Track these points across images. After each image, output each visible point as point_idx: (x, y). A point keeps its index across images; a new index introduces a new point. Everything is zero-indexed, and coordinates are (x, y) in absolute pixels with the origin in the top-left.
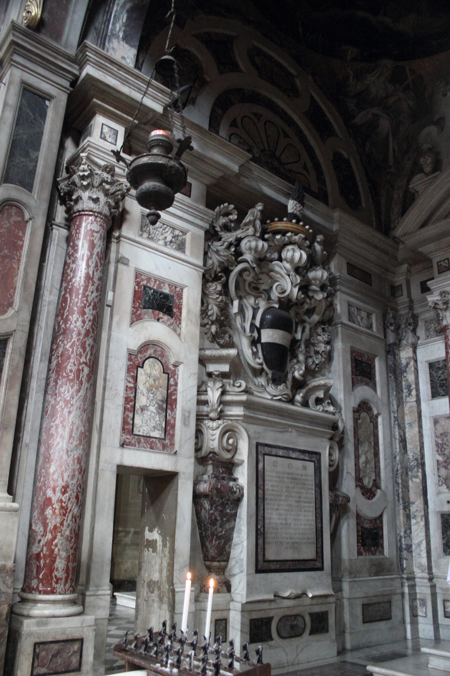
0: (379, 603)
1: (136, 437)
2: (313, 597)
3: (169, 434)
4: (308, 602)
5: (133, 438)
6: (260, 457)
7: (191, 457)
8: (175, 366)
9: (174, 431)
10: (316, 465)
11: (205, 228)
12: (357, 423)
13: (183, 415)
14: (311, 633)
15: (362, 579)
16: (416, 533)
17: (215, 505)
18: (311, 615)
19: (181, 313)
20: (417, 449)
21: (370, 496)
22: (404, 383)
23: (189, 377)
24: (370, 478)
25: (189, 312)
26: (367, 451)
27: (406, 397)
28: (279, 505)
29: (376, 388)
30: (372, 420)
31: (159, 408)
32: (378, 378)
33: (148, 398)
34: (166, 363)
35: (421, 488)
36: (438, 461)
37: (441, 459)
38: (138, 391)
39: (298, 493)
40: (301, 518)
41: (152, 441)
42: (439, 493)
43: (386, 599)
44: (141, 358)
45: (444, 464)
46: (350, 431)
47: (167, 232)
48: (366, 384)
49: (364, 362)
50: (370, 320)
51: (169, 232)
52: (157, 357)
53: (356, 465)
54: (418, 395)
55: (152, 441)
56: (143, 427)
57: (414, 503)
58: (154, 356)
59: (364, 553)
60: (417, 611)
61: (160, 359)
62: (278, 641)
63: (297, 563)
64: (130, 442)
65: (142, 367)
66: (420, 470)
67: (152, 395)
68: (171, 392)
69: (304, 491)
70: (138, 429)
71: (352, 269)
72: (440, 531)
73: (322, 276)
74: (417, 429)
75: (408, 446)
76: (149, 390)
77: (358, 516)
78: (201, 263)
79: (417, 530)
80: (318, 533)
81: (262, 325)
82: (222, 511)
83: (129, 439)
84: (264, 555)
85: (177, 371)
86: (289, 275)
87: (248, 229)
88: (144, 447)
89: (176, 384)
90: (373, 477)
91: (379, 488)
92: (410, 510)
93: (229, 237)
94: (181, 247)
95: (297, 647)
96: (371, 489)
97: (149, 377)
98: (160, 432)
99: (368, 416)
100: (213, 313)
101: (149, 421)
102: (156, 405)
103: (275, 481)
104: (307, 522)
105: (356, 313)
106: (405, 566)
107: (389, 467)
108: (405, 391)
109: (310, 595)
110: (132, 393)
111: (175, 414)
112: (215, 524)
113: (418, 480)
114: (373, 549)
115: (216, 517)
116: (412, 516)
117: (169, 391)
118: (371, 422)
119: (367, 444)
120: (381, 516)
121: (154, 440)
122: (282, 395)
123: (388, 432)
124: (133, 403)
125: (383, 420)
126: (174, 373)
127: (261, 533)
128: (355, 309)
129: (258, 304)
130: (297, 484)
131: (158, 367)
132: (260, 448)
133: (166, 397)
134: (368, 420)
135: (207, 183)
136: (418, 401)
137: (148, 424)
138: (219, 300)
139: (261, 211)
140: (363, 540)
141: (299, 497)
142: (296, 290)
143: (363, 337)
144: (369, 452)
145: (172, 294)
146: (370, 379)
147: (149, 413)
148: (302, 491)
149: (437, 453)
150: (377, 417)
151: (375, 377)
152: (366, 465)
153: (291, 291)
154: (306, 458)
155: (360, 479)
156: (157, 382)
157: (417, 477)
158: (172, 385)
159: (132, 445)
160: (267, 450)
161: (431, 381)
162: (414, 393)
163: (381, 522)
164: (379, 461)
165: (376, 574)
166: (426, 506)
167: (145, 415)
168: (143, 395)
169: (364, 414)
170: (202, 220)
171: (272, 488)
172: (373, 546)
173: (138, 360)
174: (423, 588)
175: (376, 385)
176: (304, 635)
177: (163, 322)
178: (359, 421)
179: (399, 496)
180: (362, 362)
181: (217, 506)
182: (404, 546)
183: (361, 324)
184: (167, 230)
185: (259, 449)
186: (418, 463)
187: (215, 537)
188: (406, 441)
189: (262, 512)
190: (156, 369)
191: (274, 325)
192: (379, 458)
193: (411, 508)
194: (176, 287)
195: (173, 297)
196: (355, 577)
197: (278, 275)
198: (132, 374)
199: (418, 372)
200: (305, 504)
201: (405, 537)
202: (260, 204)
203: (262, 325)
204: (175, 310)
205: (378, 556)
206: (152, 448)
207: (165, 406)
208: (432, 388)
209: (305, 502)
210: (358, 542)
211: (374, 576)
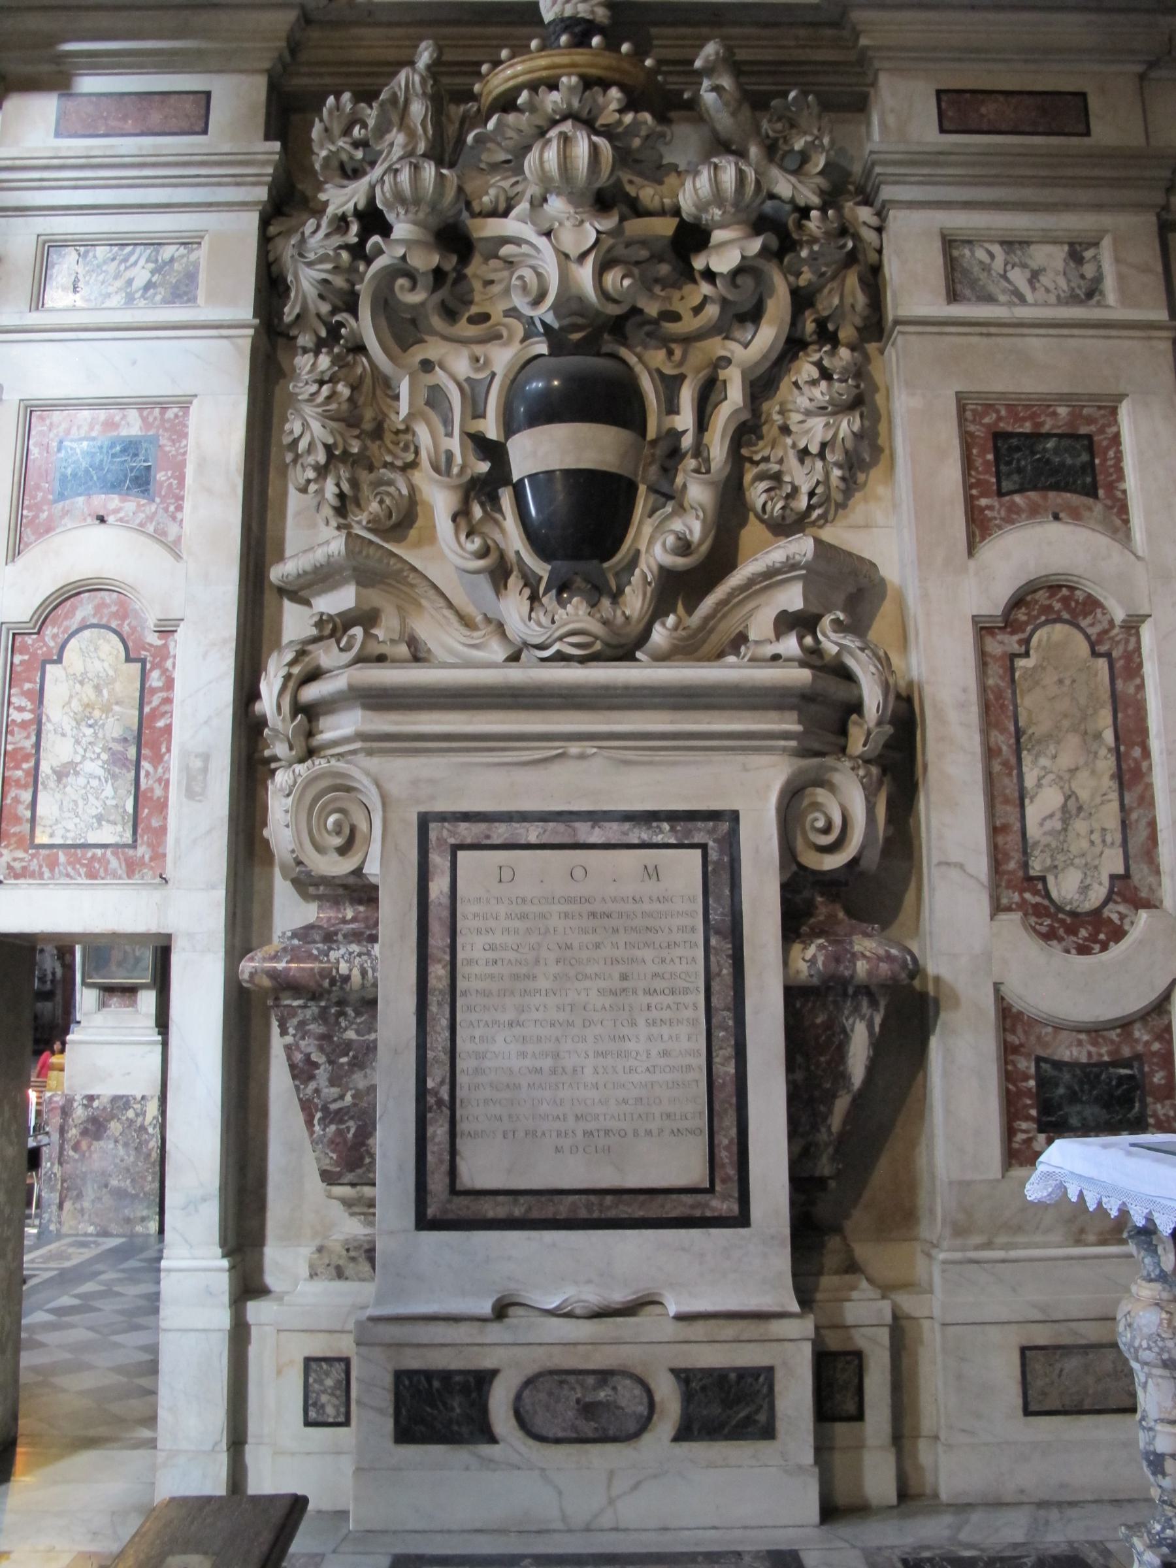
1: (43, 852)
2: (681, 1318)
3: (149, 828)
4: (671, 1330)
5: (33, 856)
6: (439, 861)
7: (213, 887)
8: (166, 630)
9: (165, 818)
10: (713, 855)
11: (256, 203)
12: (1012, 669)
13: (186, 769)
14: (684, 1434)
15: (1013, 1254)
17: (295, 1021)
18: (684, 1376)
19: (181, 479)
21: (1093, 938)
23: (205, 655)
24: (1090, 869)
25: (202, 464)
26: (1073, 771)
28: (522, 1009)
29: (1126, 522)
30: (1103, 648)
31: (114, 763)
32: (1132, 482)
33: (78, 742)
34: (133, 629)
38: (47, 727)
39: (615, 961)
40: (631, 1046)
41: (94, 856)
44: (54, 637)
46: (962, 706)
47: (136, 263)
48: (1056, 517)
49: (1049, 436)
50: (1089, 270)
51: (142, 262)
52: (104, 621)
53: (995, 830)
55: (94, 856)
56: (64, 823)
58: (95, 621)
61: (114, 625)
62: (523, 1449)
63: (609, 1199)
64: (24, 868)
65: (59, 660)
67: (90, 731)
68: (153, 710)
69: (648, 954)
70: (49, 830)
71: (958, 109)
73: (716, 183)
76: (83, 718)
78: (245, 311)
80: (719, 1096)
81: (510, 427)
82: (326, 1037)
83: (22, 860)
84: (453, 1172)
85: (171, 645)
86: (548, 234)
87: (392, 145)
88: (68, 875)
89: (169, 684)
93: (342, 198)
94: (182, 292)
95: (611, 1474)
96: (1097, 912)
97: (82, 683)
98: (119, 828)
99: (1079, 637)
100: (311, 445)
101: (81, 803)
102: (104, 756)
103: (507, 931)
104: (662, 1062)
105: (998, 264)
109: (672, 1309)
110: (28, 737)
111: (167, 770)
112: (312, 1077)
115: (308, 1056)
117: (147, 709)
118: (1095, 654)
119: (1073, 740)
121: (99, 852)
122: (560, 639)
124: (32, 763)
126: (162, 654)
127: (440, 1102)
128: (996, 249)
129: (487, 362)
130: (616, 930)
131: (111, 646)
132: (434, 830)
133: (135, 727)
134: (1084, 648)
135: (267, 65)
137: (80, 811)
138: (320, 399)
139: (435, 69)
141: (624, 977)
142: (585, 275)
143: (1035, 344)
144: (1083, 775)
145: (151, 433)
146: (1091, 491)
147: (82, 781)
148: (639, 953)
150: (1133, 625)
151: (1121, 477)
152: (1066, 821)
153: (565, 278)
154: (659, 839)
155: (1030, 879)
156: (105, 692)
158: (154, 691)
159: (32, 875)
160: (467, 832)
164: (1147, 801)
167: (68, 789)
168: (63, 735)
170: (238, 184)
171: (491, 955)
173: (46, 644)
176: (647, 1438)
177: (121, 520)
178: (1021, 663)
180: (1037, 437)
181: (302, 1024)
183: (1030, 297)
184: (133, 259)
185: (433, 836)
187: (319, 1115)
189: (447, 1034)
190: (103, 656)
191: (546, 411)
192: (1149, 786)
194: (164, 410)
195: (153, 441)
196: (988, 1245)
197: (525, 248)
198: (27, 686)
200: (655, 1000)
202: (423, 45)
203: (510, 427)
204: (161, 476)
206: (92, 875)
207: (132, 752)
209: (649, 992)
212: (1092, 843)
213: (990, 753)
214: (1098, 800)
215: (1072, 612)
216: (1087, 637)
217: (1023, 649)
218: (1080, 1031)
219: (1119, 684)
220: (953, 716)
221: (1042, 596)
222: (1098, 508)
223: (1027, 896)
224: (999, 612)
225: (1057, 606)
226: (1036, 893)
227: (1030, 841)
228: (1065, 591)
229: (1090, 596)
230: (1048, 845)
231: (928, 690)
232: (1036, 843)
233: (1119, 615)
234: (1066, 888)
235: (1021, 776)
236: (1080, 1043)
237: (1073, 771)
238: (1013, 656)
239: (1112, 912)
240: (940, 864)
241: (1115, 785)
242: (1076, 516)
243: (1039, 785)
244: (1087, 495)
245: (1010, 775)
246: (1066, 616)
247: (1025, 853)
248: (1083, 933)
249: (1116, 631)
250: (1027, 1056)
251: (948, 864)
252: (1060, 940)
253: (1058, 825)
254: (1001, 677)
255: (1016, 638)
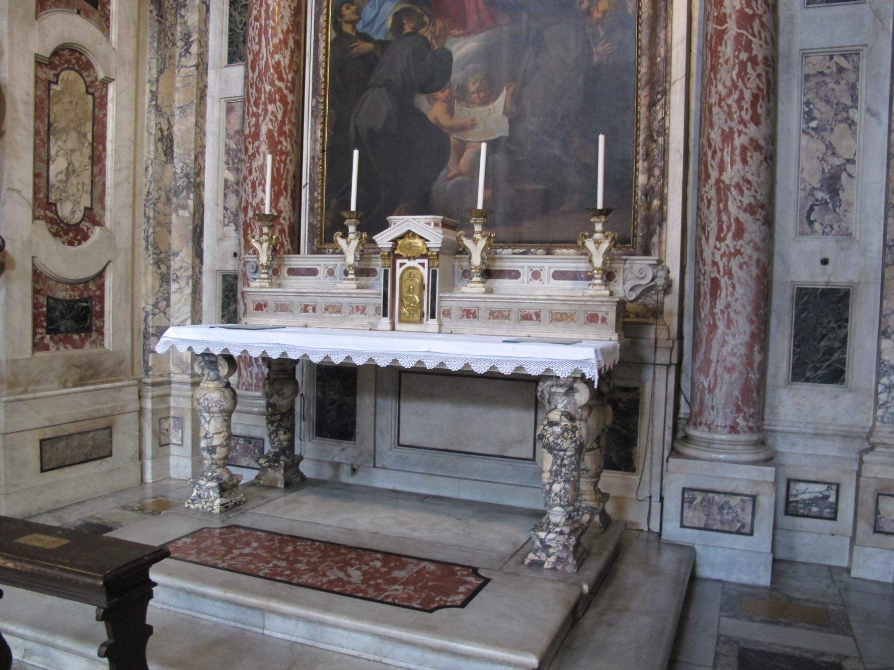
0: (82, 433)
12: (49, 89)
16: (177, 307)
20: (189, 155)
21: (75, 238)
22: (179, 28)
24: (77, 203)
26: (73, 151)
27: (180, 56)
29: (108, 27)
30: (92, 90)
35: (191, 227)
36: (226, 181)
37: (231, 177)
42: (220, 240)
43: (102, 423)
45: (235, 187)
46: (26, 103)
48: (79, 13)
53: (36, 175)
54: (202, 57)
57: (176, 254)
59: (51, 344)
60: (169, 436)
66: (192, 196)
72: (219, 304)
74: (192, 119)
75: (176, 150)
77: (38, 276)
79: (179, 301)
90: (86, 202)
91: (99, 224)
92: (169, 267)
96: (78, 225)
99: (82, 81)
106: (150, 364)
107: (127, 187)
108: (180, 44)
113: (186, 214)
114: (76, 337)
116: (173, 277)
118: (88, 92)
119: (74, 135)
120: (101, 275)
123: (129, 117)
125: (119, 93)
134: (83, 88)
136: (202, 67)
140: (50, 321)
144: (77, 154)
149: (225, 166)
150: (106, 82)
152: (67, 176)
155: (49, 204)
157: (185, 207)
161: (230, 30)
162: (194, 49)
163: (101, 287)
164: (103, 172)
165: (81, 381)
166: (197, 261)
169: (69, 75)
172: (78, 331)
174: (181, 399)
175: (108, 20)
178: (54, 87)
179: (147, 241)
182: (151, 330)
186: (190, 182)
188: (172, 141)
192: (104, 165)
193: (172, 263)
196: (25, 392)
199: (208, 10)
201: (154, 314)
205: (88, 350)
208: (231, 43)
210: (36, 325)
211: (75, 386)
212: (78, 190)
213: (37, 133)
214: (82, 168)
215: (79, 66)
216: (85, 82)
217: (55, 80)
218: (67, 284)
219: (97, 110)
220: (21, 107)
221: (66, 53)
222: (97, 14)
223: (48, 212)
224: (48, 55)
225: (73, 61)
226: (52, 212)
227: (51, 184)
228: (77, 54)
229: (89, 61)
230: (58, 188)
231: (9, 89)
232: (54, 185)
233: (101, 75)
234: (65, 211)
235: (49, 148)
236: (67, 290)
237: (73, 151)
238: (50, 82)
239: (84, 226)
240: (9, 189)
241: (90, 163)
242: (87, 15)
243: (57, 155)
244: (93, 5)
245: (44, 146)
246: (77, 68)
247: (48, 190)
248: (71, 235)
249: (98, 83)
250: (43, 295)
251: (13, 190)
252: (61, 237)
253: (64, 179)
254: (44, 92)
255: (52, 72)
